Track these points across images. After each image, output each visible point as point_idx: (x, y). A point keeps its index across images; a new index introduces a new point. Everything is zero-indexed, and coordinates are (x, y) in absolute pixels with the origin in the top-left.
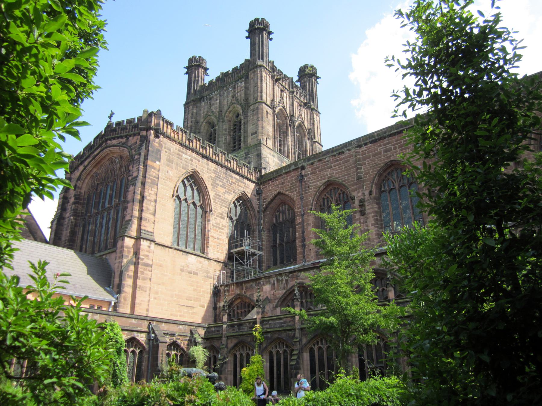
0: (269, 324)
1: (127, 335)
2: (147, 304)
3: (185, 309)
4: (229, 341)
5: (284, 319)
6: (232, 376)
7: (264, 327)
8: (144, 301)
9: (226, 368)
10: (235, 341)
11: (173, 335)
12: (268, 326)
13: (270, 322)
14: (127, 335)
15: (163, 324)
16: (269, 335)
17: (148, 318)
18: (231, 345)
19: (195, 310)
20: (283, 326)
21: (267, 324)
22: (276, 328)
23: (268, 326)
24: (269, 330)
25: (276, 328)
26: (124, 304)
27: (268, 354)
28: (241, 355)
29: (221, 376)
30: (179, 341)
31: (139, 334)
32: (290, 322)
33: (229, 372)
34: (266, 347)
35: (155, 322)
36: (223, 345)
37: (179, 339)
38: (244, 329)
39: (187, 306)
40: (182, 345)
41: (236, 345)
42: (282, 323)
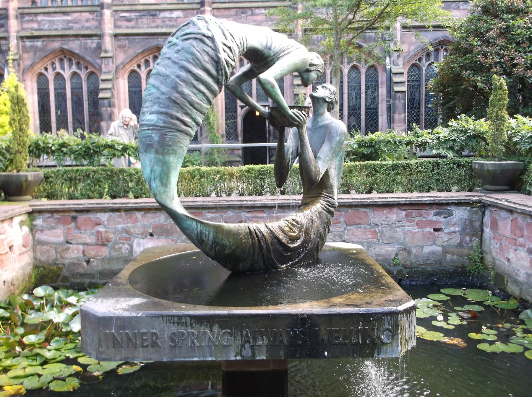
0: (38, 22)
5: (76, 15)
7: (25, 26)
12: (35, 26)
13: (40, 18)
16: (39, 43)
20: (71, 28)
21: (32, 21)
22: (56, 29)
23: (35, 26)
24: (36, 33)
25: (56, 30)
27: (35, 79)
32: (87, 20)
34: (32, 66)
42: (69, 22)
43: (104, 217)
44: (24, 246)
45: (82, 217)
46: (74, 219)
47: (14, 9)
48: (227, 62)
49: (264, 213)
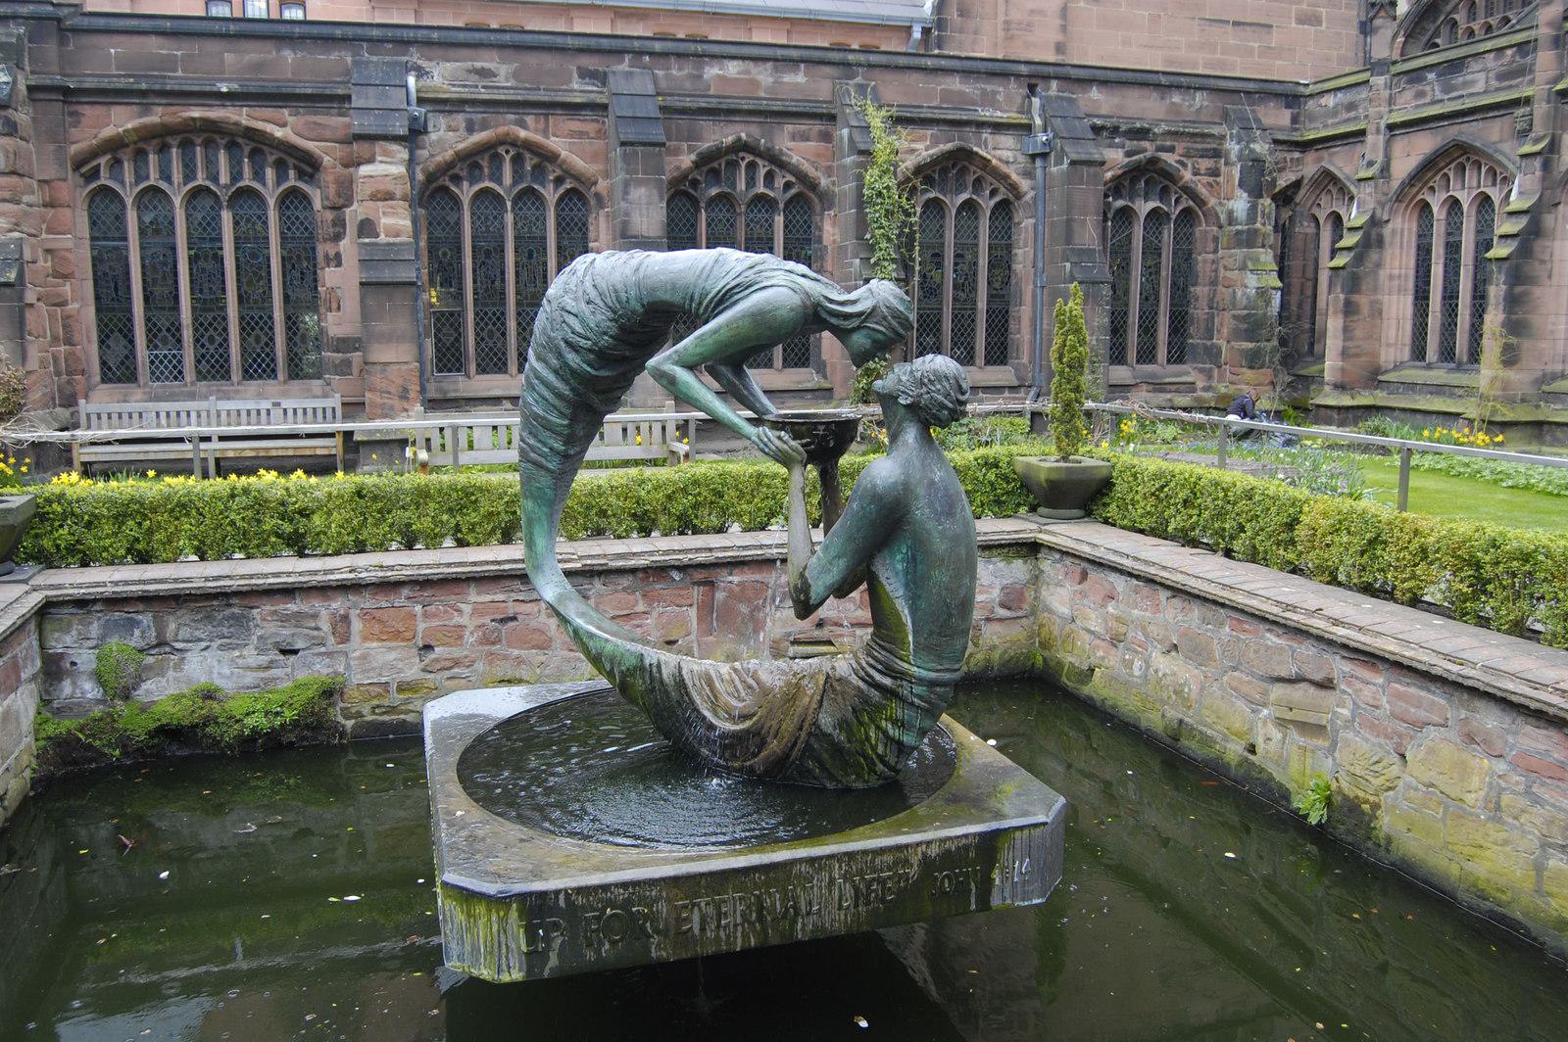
1: (935, 142)
2: (1058, 22)
3: (1230, 37)
4: (1400, 145)
6: (1410, 299)
8: (1041, 12)
9: (1378, 265)
10: (1423, 145)
11: (1142, 134)
14: (935, 142)
15: (1095, 93)
17: (1024, 69)
18: (1404, 164)
19: (1275, 37)
26: (961, 31)
28: (1454, 204)
29: (1356, 298)
30: (1170, 158)
31: (986, 134)
33: (1396, 283)
35: (1054, 84)
36: (1370, 164)
37: (1171, 150)
38: (1473, 82)
39: (1236, 24)
40: (1187, 176)
41: (1430, 166)
43: (1120, 583)
44: (1003, 605)
45: (1094, 575)
46: (1084, 576)
47: (1550, 24)
48: (567, 342)
49: (1377, 671)
